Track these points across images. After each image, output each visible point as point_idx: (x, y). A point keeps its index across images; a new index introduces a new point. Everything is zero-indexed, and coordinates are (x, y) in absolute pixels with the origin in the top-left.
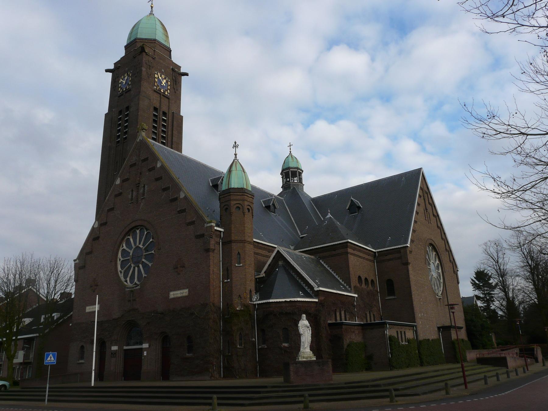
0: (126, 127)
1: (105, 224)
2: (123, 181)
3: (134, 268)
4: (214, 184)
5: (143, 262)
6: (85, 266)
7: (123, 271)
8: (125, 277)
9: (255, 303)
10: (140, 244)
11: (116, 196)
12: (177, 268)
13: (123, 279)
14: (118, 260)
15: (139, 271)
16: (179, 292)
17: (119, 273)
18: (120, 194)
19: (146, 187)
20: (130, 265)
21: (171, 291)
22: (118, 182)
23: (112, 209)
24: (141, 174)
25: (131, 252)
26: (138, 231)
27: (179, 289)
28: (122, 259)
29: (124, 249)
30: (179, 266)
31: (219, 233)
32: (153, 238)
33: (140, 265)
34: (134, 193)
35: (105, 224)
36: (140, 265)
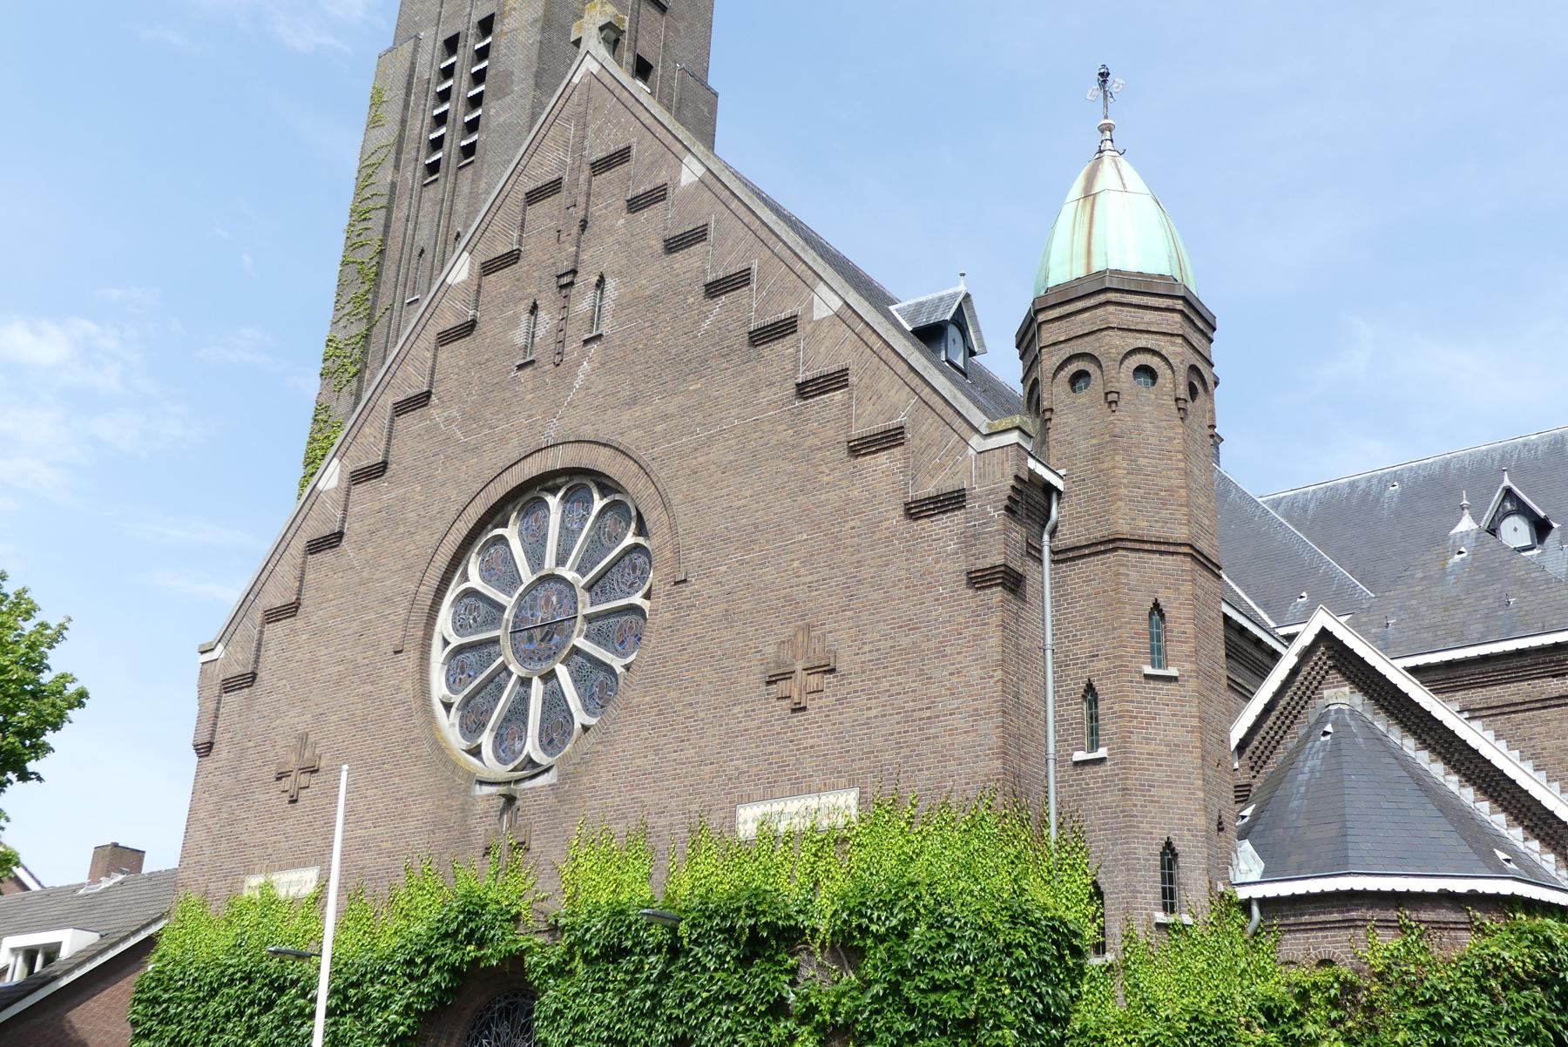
0: (476, 102)
1: (377, 471)
2: (489, 268)
3: (525, 682)
4: (923, 321)
5: (576, 651)
6: (254, 676)
7: (457, 699)
8: (472, 728)
9: (1243, 894)
10: (561, 561)
11: (447, 338)
12: (786, 676)
13: (456, 741)
14: (437, 642)
15: (554, 701)
16: (794, 805)
17: (439, 710)
18: (469, 328)
19: (610, 284)
20: (504, 668)
21: (750, 800)
22: (461, 271)
23: (422, 400)
24: (584, 225)
25: (509, 601)
26: (553, 501)
27: (799, 788)
28: (456, 641)
29: (471, 593)
30: (799, 667)
31: (1039, 497)
32: (641, 530)
33: (562, 672)
34: (542, 315)
35: (377, 471)
36: (562, 672)
